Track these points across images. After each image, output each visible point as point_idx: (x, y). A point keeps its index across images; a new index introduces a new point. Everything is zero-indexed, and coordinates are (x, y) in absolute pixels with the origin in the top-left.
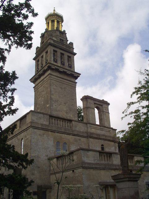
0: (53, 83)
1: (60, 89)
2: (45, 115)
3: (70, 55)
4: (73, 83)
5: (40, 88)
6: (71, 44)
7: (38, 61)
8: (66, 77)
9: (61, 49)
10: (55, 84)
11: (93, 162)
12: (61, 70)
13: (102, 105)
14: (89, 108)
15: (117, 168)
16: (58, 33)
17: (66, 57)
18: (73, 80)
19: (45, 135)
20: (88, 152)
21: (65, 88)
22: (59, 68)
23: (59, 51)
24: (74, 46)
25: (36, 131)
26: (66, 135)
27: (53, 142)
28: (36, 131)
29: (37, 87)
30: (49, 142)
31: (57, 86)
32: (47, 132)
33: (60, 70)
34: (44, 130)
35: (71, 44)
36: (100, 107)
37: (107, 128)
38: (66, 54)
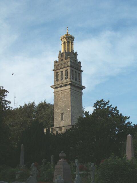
3: (79, 72)
4: (80, 93)
5: (61, 95)
6: (80, 63)
8: (77, 90)
9: (75, 69)
12: (76, 85)
16: (73, 55)
17: (78, 74)
18: (79, 90)
23: (75, 70)
24: (82, 65)
29: (57, 93)
33: (76, 85)
35: (80, 63)
38: (78, 72)
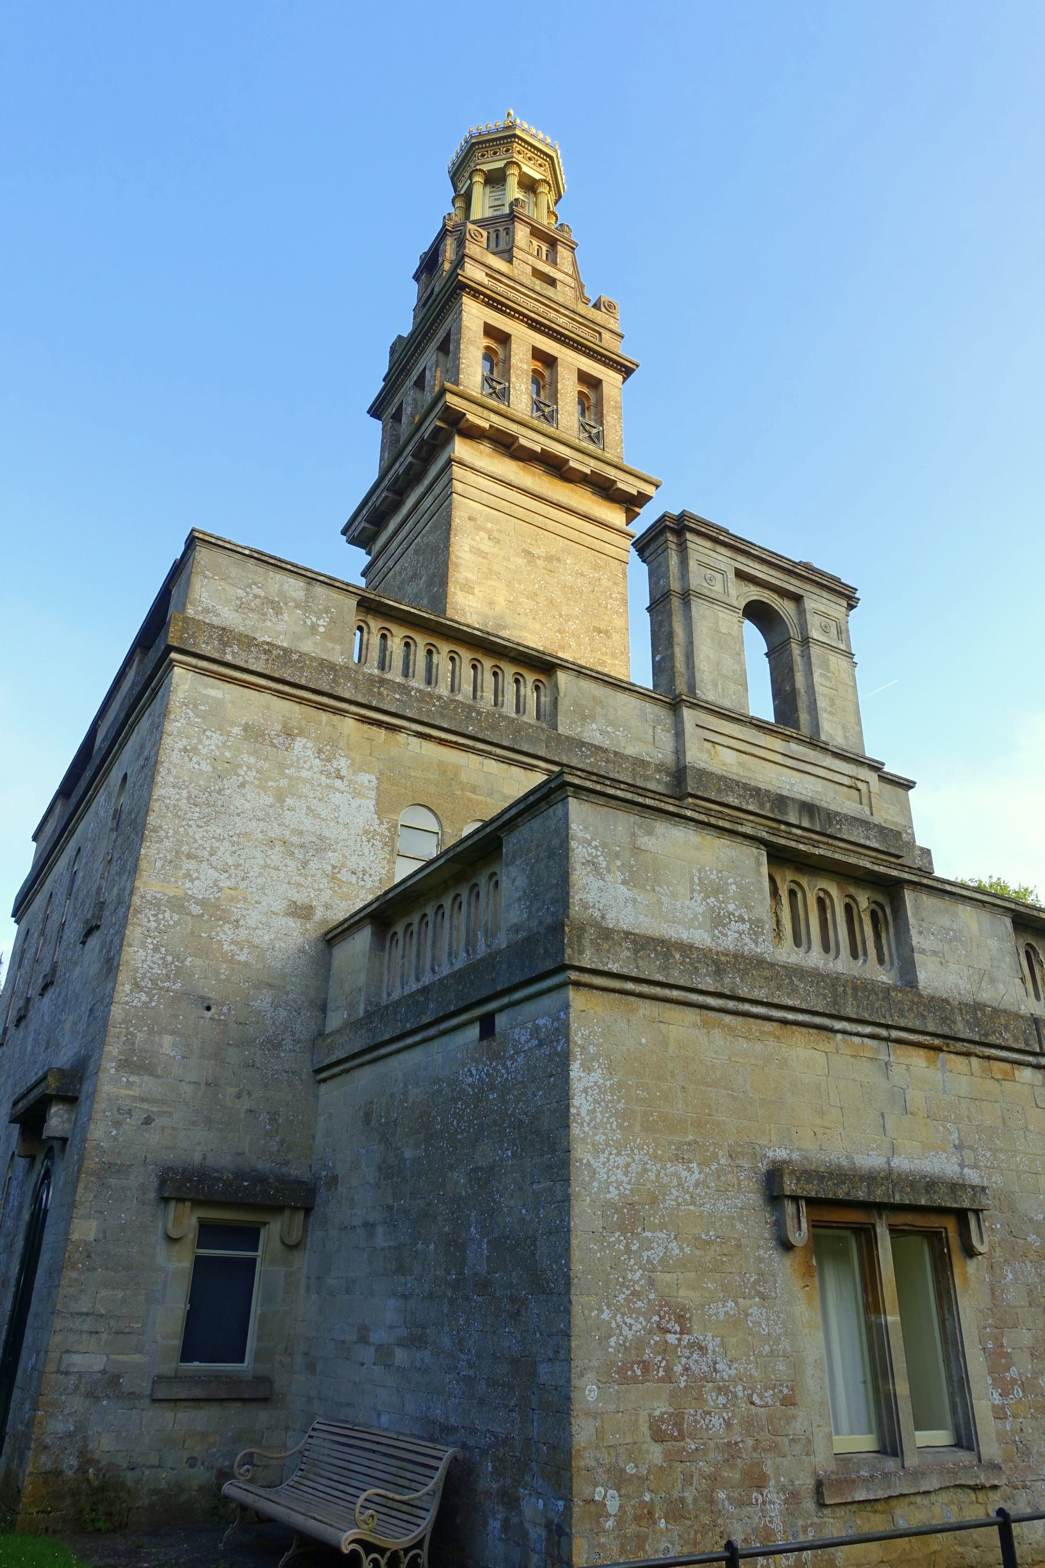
0: (470, 519)
1: (521, 561)
2: (319, 590)
7: (397, 417)
9: (535, 325)
10: (489, 525)
11: (701, 937)
13: (797, 599)
14: (701, 596)
15: (961, 1029)
19: (299, 742)
20: (650, 833)
21: (549, 559)
22: (513, 428)
25: (212, 692)
26: (492, 765)
27: (371, 804)
28: (212, 692)
30: (337, 798)
31: (498, 542)
32: (324, 717)
34: (301, 701)
36: (785, 608)
37: (836, 755)
